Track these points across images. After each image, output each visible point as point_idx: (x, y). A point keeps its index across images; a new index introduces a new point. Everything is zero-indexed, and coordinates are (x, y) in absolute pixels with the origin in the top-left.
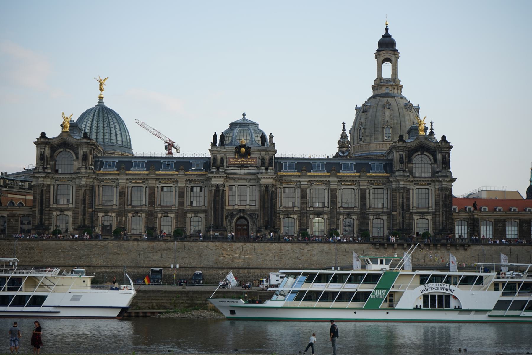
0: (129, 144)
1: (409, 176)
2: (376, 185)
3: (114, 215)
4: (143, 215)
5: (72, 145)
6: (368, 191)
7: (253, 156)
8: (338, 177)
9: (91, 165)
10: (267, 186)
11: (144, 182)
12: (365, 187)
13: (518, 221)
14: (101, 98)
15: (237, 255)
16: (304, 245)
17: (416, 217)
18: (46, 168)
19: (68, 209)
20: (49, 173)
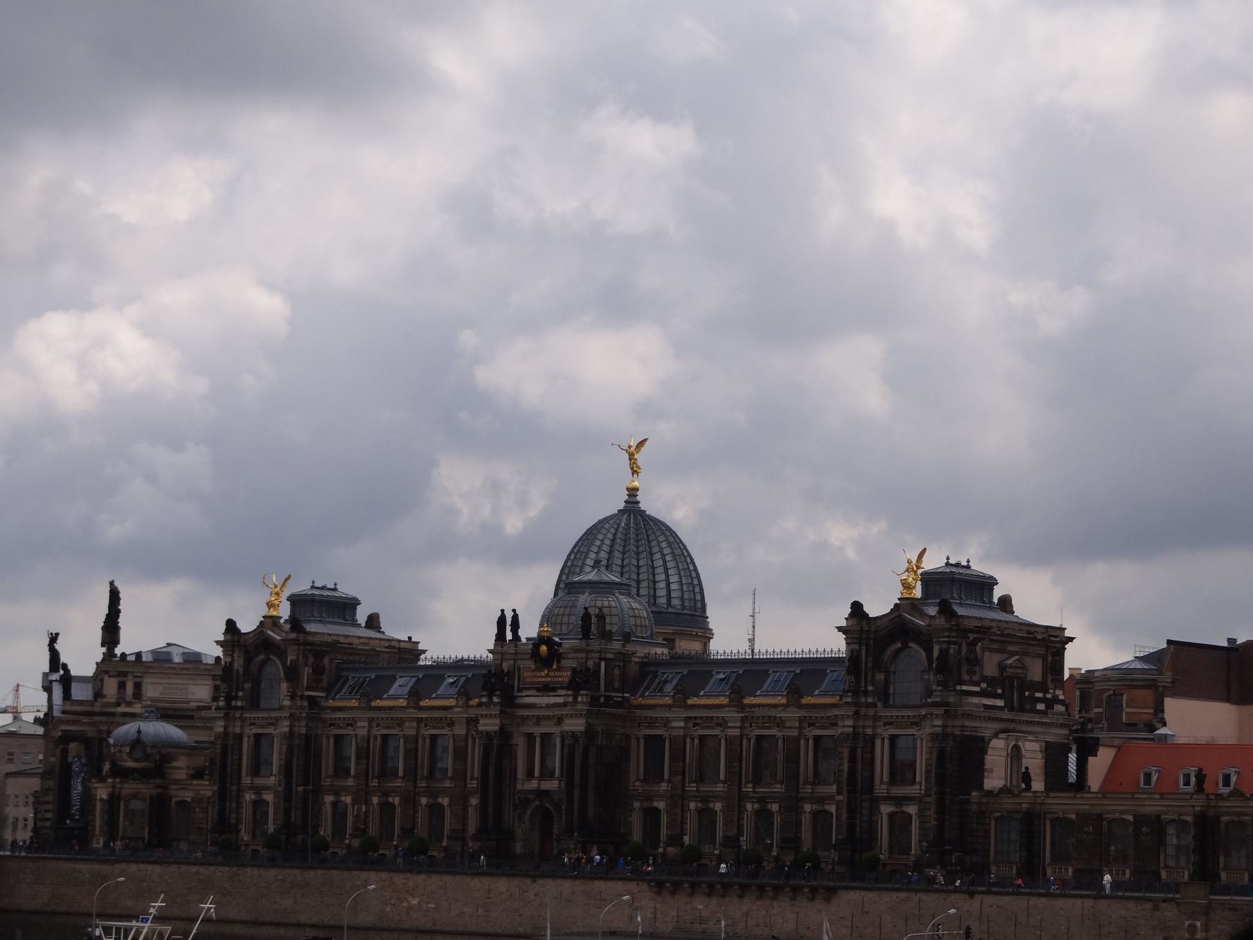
0: (699, 605)
1: (874, 705)
2: (818, 728)
3: (348, 800)
4: (397, 801)
5: (278, 647)
6: (803, 741)
7: (565, 663)
8: (742, 708)
9: (308, 689)
10: (574, 735)
11: (399, 725)
12: (795, 733)
13: (1130, 818)
14: (633, 492)
15: (415, 902)
16: (528, 881)
17: (886, 809)
18: (236, 698)
19: (267, 788)
20: (242, 708)
